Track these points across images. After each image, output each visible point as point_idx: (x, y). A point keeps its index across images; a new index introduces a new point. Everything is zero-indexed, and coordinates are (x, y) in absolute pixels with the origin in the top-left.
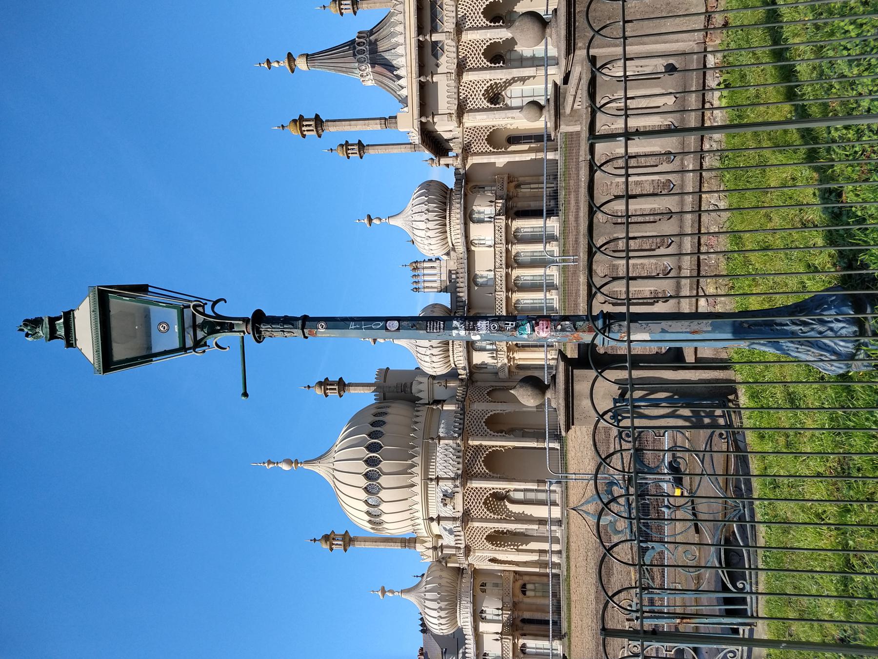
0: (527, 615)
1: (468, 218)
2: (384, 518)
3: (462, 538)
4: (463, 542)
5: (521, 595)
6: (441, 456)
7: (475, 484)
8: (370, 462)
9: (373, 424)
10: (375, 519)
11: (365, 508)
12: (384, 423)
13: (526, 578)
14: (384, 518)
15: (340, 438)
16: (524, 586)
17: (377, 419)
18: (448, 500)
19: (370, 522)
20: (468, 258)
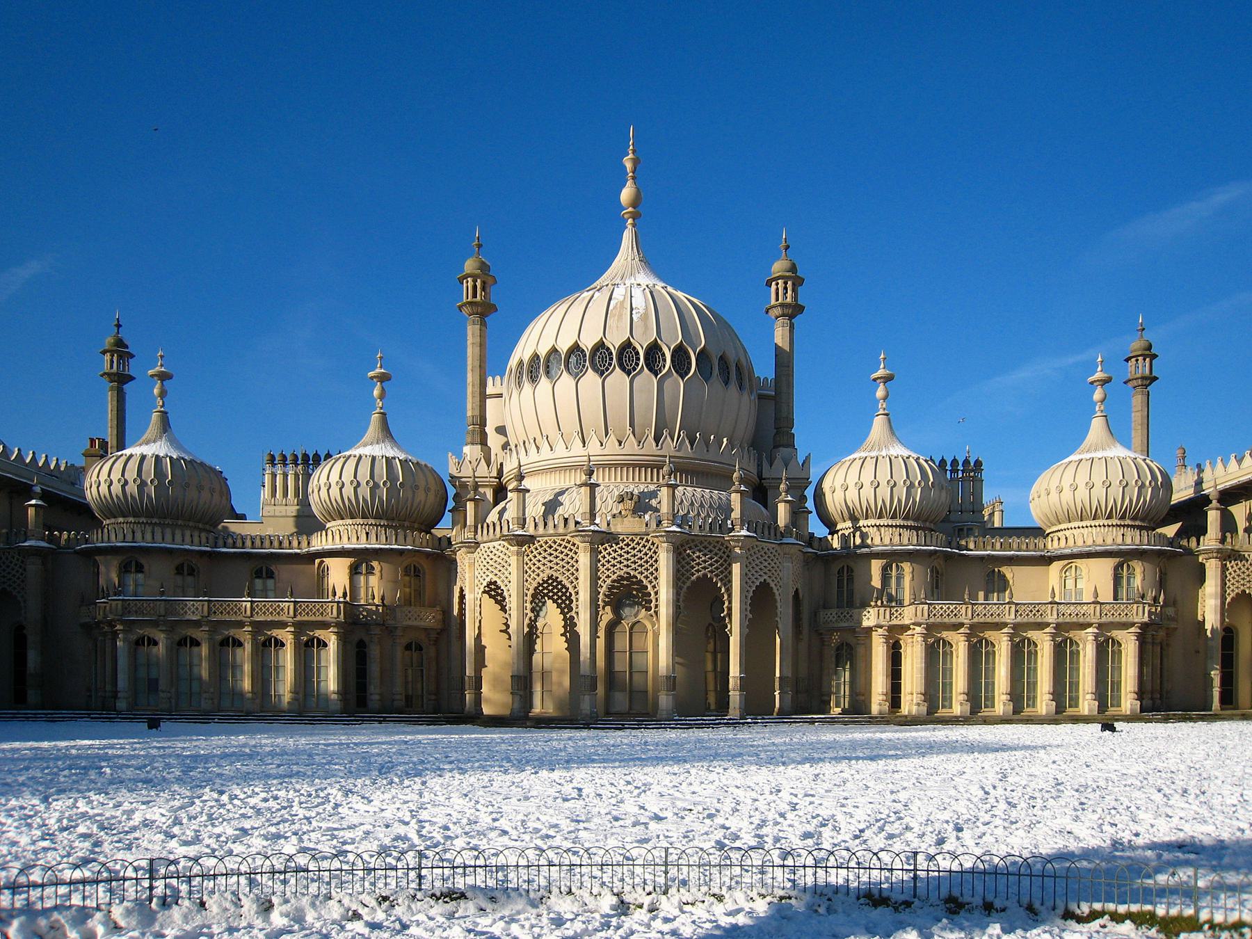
0: (374, 651)
1: (1123, 557)
2: (544, 382)
3: (551, 531)
4: (485, 538)
5: (405, 641)
6: (689, 495)
7: (665, 561)
8: (653, 351)
9: (723, 359)
10: (536, 368)
11: (543, 352)
12: (726, 383)
13: (432, 652)
14: (544, 382)
15: (695, 300)
17: (733, 369)
18: (629, 504)
19: (536, 357)
20: (1042, 557)
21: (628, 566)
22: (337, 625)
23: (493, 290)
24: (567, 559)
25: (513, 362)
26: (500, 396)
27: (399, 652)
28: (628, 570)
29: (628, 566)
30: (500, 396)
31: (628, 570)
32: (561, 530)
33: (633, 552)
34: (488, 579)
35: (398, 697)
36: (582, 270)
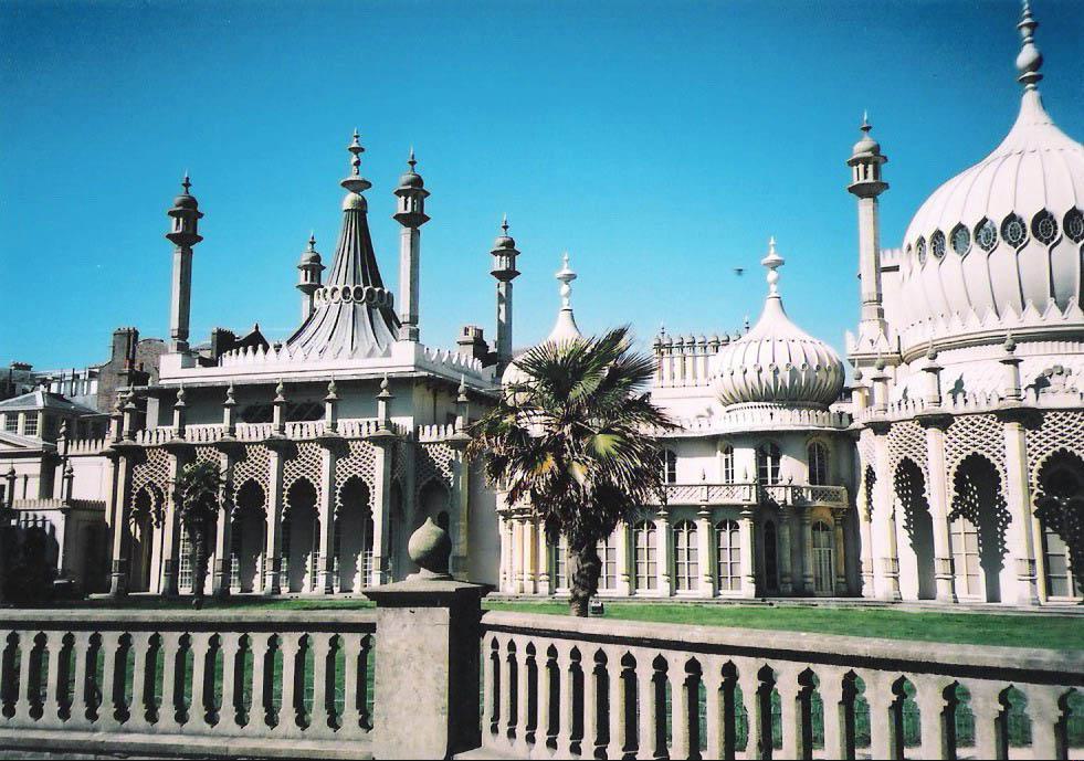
16: (825, 528)
21: (1063, 442)
22: (751, 507)
23: (884, 167)
24: (992, 436)
25: (911, 237)
26: (896, 268)
27: (808, 531)
28: (1064, 446)
29: (1063, 442)
30: (896, 268)
31: (1064, 446)
32: (984, 408)
33: (1061, 424)
34: (902, 457)
35: (810, 580)
36: (984, 134)
